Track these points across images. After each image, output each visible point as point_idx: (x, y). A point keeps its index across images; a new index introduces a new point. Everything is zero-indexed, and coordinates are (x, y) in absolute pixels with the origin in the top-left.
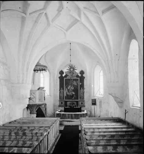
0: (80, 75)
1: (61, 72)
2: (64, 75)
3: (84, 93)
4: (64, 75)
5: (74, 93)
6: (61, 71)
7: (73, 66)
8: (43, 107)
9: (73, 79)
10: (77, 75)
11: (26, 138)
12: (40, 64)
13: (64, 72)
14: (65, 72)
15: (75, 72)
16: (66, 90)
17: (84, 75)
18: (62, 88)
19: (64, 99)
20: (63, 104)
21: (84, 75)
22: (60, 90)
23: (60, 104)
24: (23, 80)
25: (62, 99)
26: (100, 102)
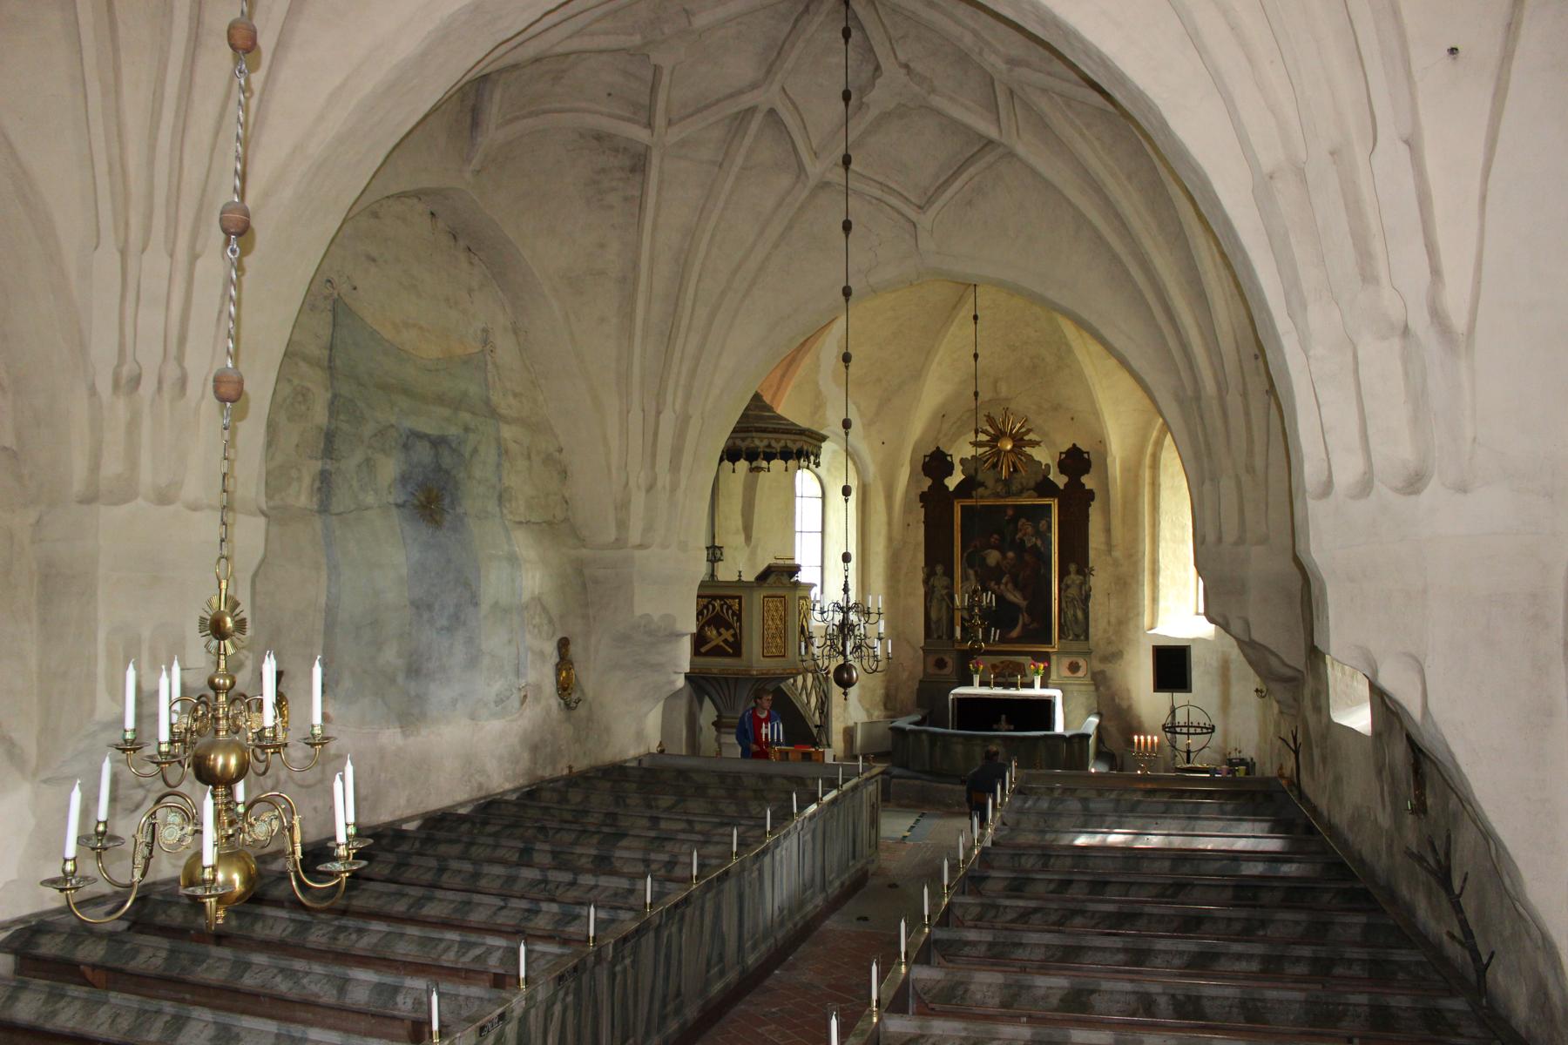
0: (1061, 481)
1: (936, 464)
2: (952, 482)
3: (1087, 597)
4: (952, 482)
5: (1014, 597)
8: (804, 686)
10: (1040, 478)
11: (596, 886)
12: (780, 418)
13: (956, 462)
14: (963, 461)
15: (1030, 457)
16: (965, 578)
17: (1088, 481)
18: (939, 569)
20: (948, 670)
22: (926, 582)
23: (931, 670)
24: (648, 529)
25: (940, 637)
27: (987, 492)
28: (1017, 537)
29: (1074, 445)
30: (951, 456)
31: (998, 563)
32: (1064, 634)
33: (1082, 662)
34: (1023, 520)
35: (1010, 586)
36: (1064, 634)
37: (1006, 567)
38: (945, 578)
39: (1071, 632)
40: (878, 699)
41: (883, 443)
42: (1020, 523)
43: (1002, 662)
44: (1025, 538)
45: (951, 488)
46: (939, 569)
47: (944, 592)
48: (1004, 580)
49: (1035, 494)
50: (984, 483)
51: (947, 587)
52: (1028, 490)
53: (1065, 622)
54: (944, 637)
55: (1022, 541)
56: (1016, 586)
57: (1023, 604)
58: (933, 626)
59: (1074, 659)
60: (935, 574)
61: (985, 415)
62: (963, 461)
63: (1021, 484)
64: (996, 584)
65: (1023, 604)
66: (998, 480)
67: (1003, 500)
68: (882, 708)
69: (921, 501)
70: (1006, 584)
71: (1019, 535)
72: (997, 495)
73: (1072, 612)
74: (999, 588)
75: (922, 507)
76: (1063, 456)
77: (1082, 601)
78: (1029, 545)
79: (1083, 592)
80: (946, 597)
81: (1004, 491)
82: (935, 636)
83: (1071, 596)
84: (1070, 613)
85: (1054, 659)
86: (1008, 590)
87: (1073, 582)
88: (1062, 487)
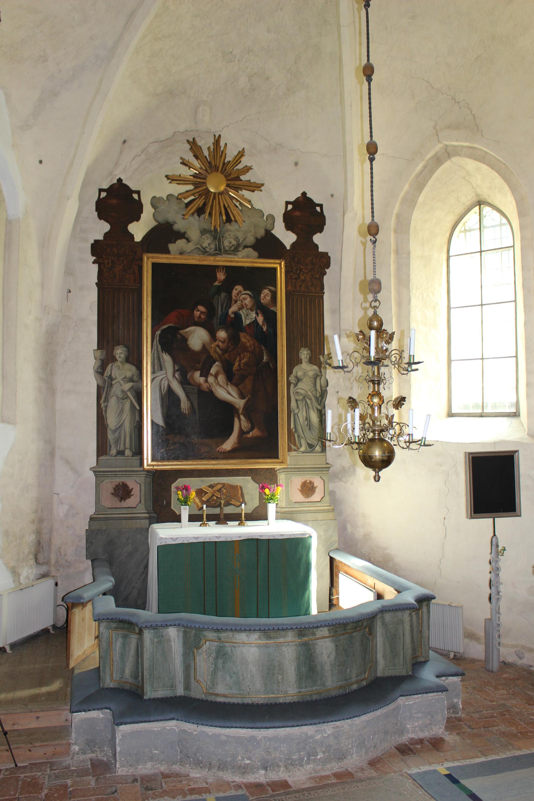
3: (324, 393)
6: (111, 190)
7: (229, 158)
9: (229, 270)
10: (261, 233)
13: (146, 201)
14: (155, 202)
16: (157, 366)
18: (120, 352)
19: (139, 452)
20: (131, 502)
21: (317, 238)
22: (101, 370)
23: (109, 501)
25: (121, 453)
26: (328, 473)
27: (190, 247)
28: (231, 310)
29: (304, 194)
30: (138, 193)
31: (204, 346)
32: (295, 445)
33: (318, 482)
34: (239, 288)
35: (221, 378)
36: (295, 445)
37: (215, 351)
38: (128, 366)
39: (303, 442)
40: (27, 551)
41: (41, 162)
42: (235, 292)
43: (211, 486)
44: (243, 313)
45: (138, 238)
46: (120, 352)
47: (127, 386)
48: (213, 371)
49: (256, 254)
50: (185, 233)
51: (131, 380)
52: (246, 247)
53: (295, 427)
54: (128, 452)
55: (237, 316)
56: (230, 378)
57: (239, 403)
58: (111, 436)
59: (308, 477)
60: (114, 360)
61: (188, 141)
63: (237, 239)
64: (201, 376)
65: (239, 403)
66: (204, 232)
67: (212, 258)
68: (32, 562)
69: (93, 255)
70: (216, 376)
71: (234, 308)
72: (204, 252)
73: (305, 414)
74: (206, 381)
75: (94, 262)
76: (290, 207)
77: (317, 399)
78: (248, 322)
80: (129, 393)
81: (213, 246)
82: (114, 451)
83: (302, 392)
84: (302, 416)
85: (282, 477)
86: (218, 384)
87: (305, 374)
88: (288, 248)
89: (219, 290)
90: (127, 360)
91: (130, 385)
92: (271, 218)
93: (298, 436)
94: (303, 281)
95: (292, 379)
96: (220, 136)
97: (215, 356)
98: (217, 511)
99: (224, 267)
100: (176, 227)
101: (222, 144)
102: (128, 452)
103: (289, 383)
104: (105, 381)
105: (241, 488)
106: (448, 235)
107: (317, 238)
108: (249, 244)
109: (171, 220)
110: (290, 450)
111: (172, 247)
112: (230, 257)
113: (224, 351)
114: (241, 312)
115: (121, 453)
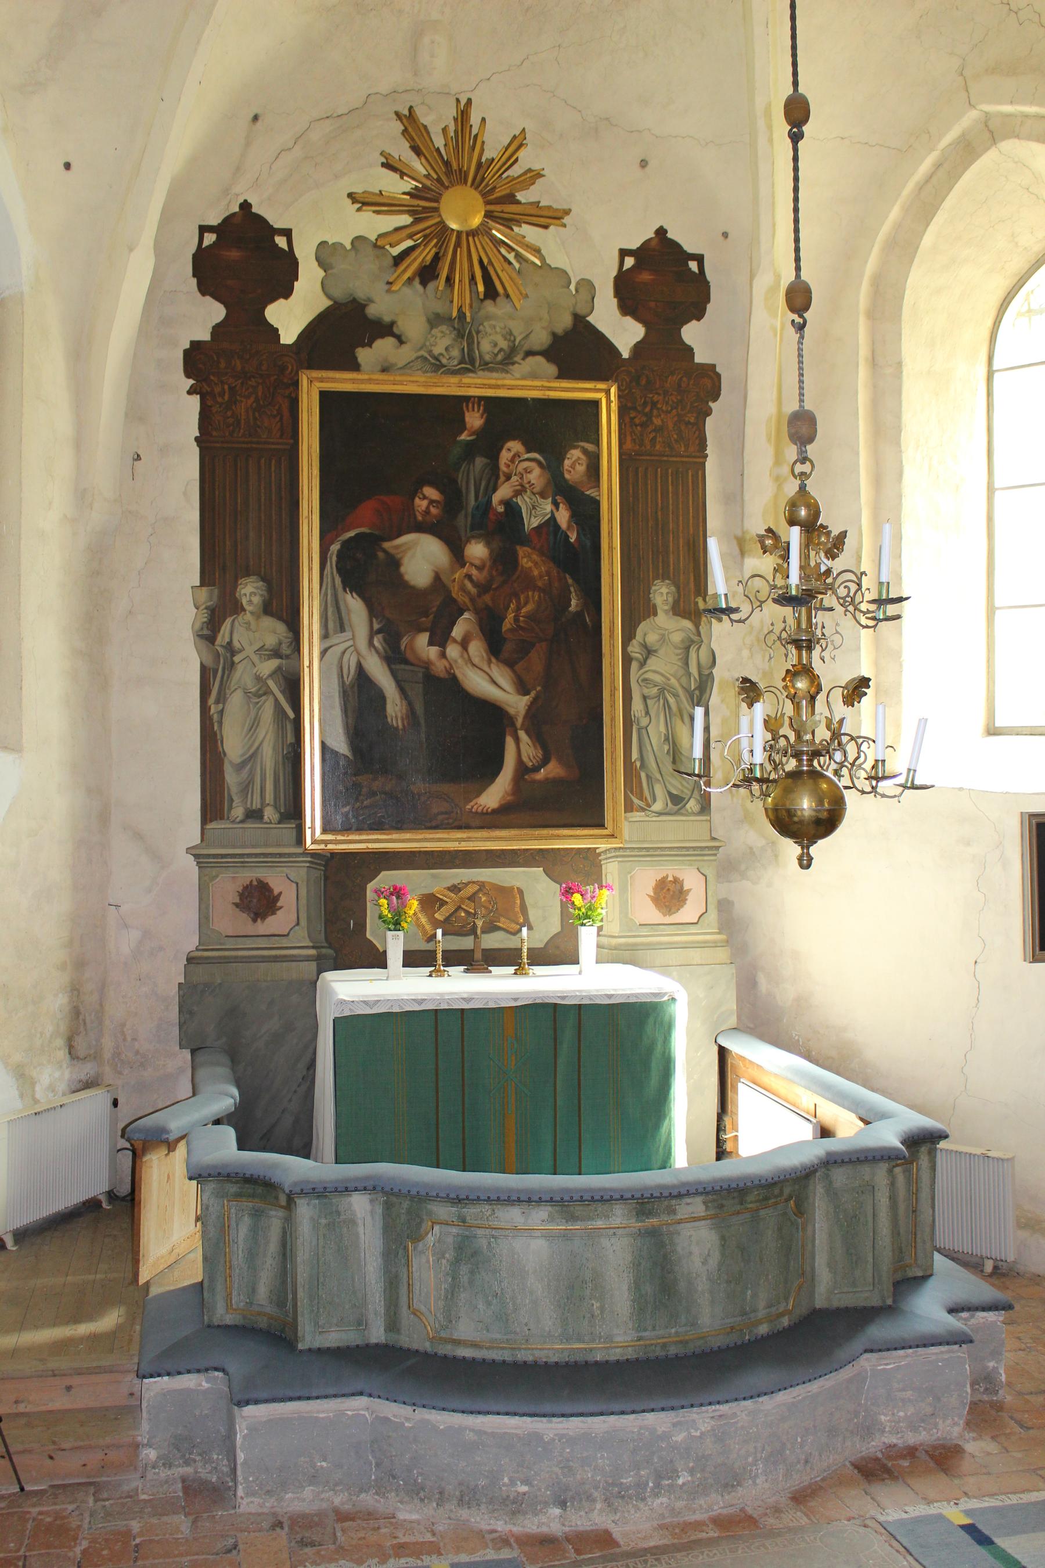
6: (226, 229)
9: (492, 405)
10: (565, 322)
13: (305, 253)
14: (325, 254)
19: (294, 812)
20: (276, 923)
21: (691, 333)
25: (254, 815)
27: (406, 354)
28: (496, 498)
29: (661, 232)
30: (287, 233)
31: (437, 577)
33: (692, 880)
34: (515, 446)
35: (477, 648)
36: (641, 797)
37: (463, 589)
38: (268, 622)
40: (50, 1029)
41: (68, 166)
42: (505, 456)
43: (455, 889)
44: (523, 502)
45: (288, 336)
47: (268, 667)
48: (457, 632)
49: (552, 369)
50: (393, 323)
52: (530, 353)
53: (642, 758)
54: (269, 813)
55: (512, 509)
56: (495, 647)
57: (517, 704)
58: (232, 779)
59: (669, 870)
60: (237, 608)
62: (325, 254)
63: (509, 335)
64: (431, 643)
65: (517, 704)
66: (435, 320)
67: (454, 379)
68: (62, 1054)
69: (188, 374)
70: (464, 644)
71: (503, 492)
72: (437, 365)
73: (662, 728)
74: (443, 655)
76: (629, 262)
78: (535, 523)
79: (694, 670)
80: (271, 683)
81: (455, 353)
82: (238, 812)
83: (658, 678)
84: (656, 731)
85: (611, 870)
87: (663, 639)
88: (626, 355)
89: (470, 451)
90: (267, 609)
91: (273, 664)
92: (587, 286)
93: (648, 777)
94: (659, 430)
95: (634, 649)
96: (469, 101)
97: (462, 598)
98: (466, 943)
99: (481, 398)
100: (372, 311)
101: (475, 119)
102: (269, 813)
103: (627, 660)
104: (217, 655)
105: (521, 892)
106: (989, 323)
107: (691, 333)
108: (537, 347)
109: (361, 295)
110: (629, 807)
111: (363, 355)
112: (493, 378)
113: (484, 588)
114: (519, 500)
115: (254, 815)
